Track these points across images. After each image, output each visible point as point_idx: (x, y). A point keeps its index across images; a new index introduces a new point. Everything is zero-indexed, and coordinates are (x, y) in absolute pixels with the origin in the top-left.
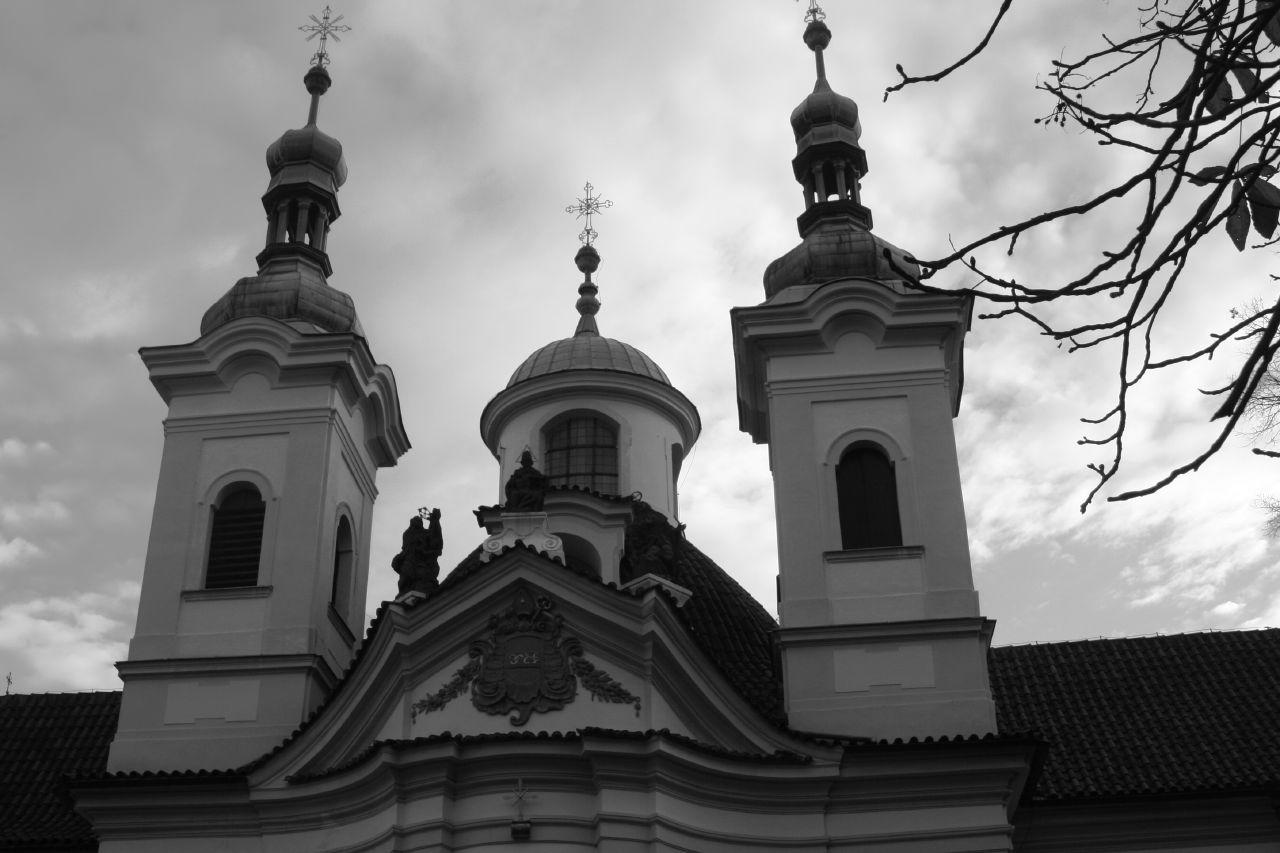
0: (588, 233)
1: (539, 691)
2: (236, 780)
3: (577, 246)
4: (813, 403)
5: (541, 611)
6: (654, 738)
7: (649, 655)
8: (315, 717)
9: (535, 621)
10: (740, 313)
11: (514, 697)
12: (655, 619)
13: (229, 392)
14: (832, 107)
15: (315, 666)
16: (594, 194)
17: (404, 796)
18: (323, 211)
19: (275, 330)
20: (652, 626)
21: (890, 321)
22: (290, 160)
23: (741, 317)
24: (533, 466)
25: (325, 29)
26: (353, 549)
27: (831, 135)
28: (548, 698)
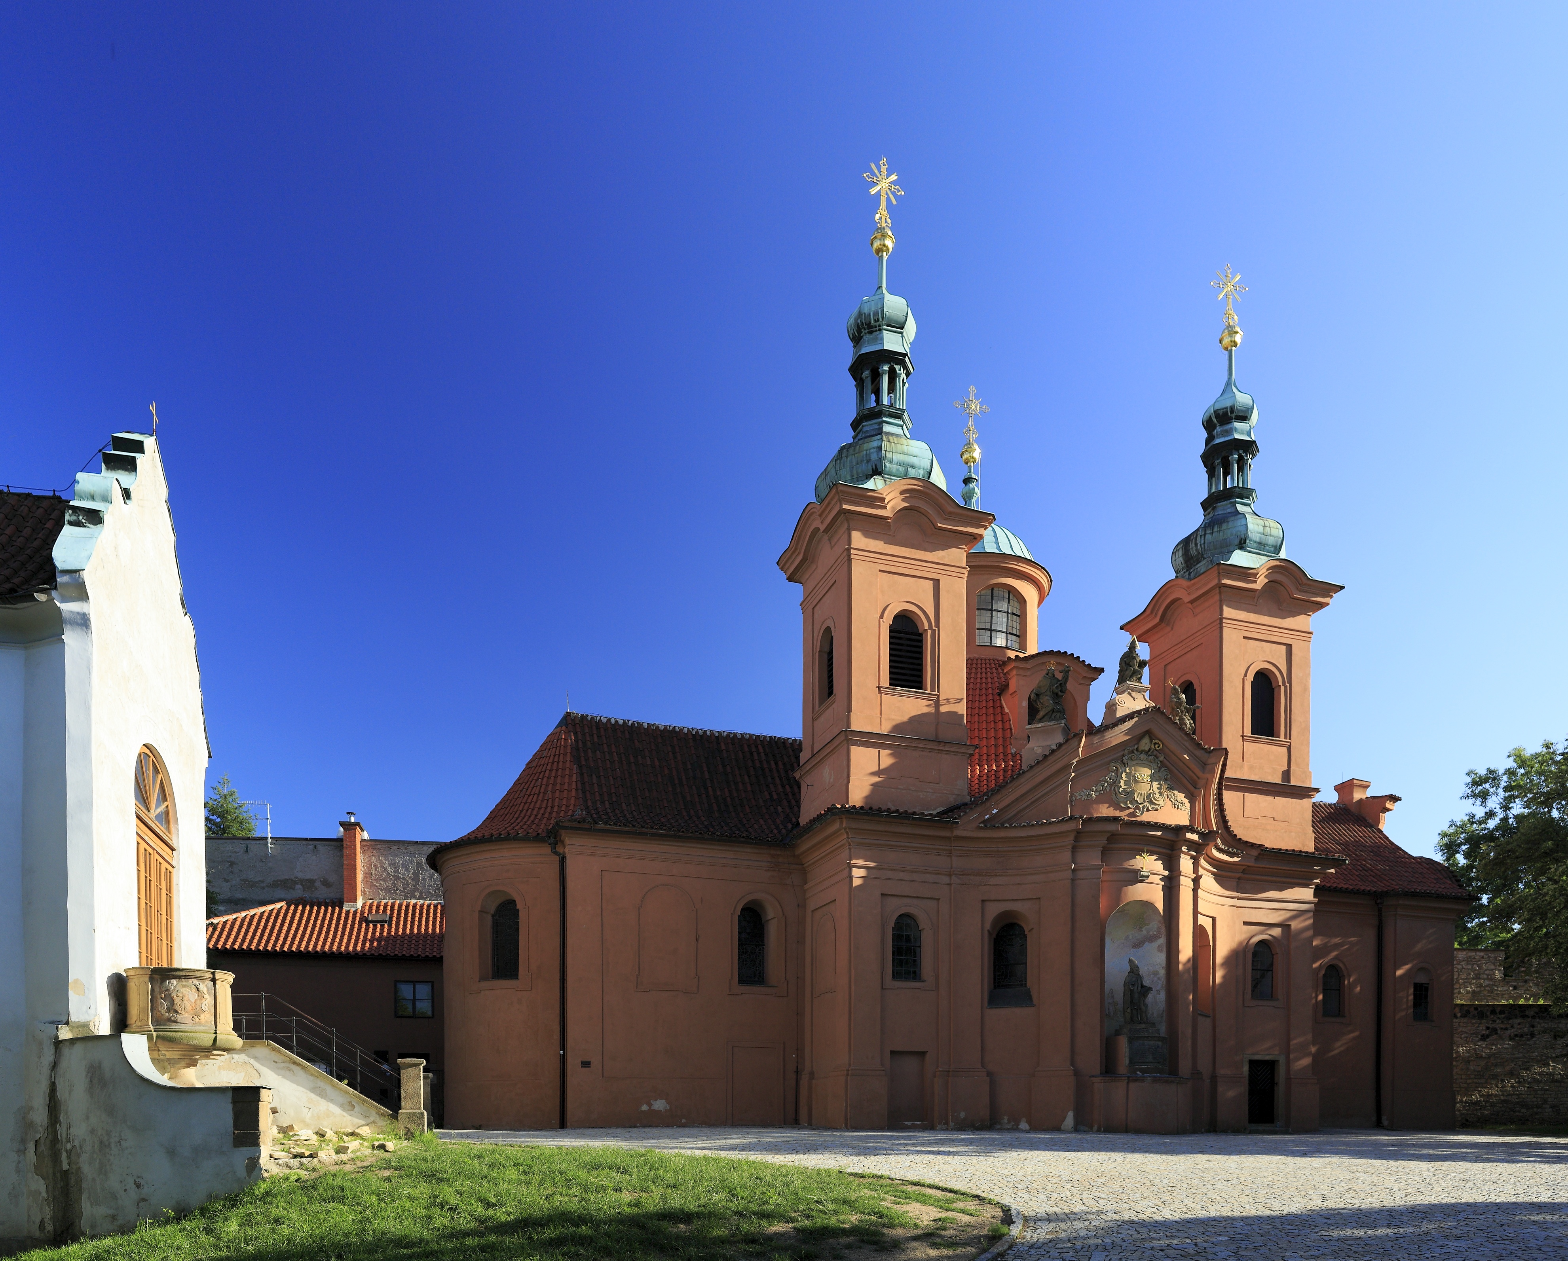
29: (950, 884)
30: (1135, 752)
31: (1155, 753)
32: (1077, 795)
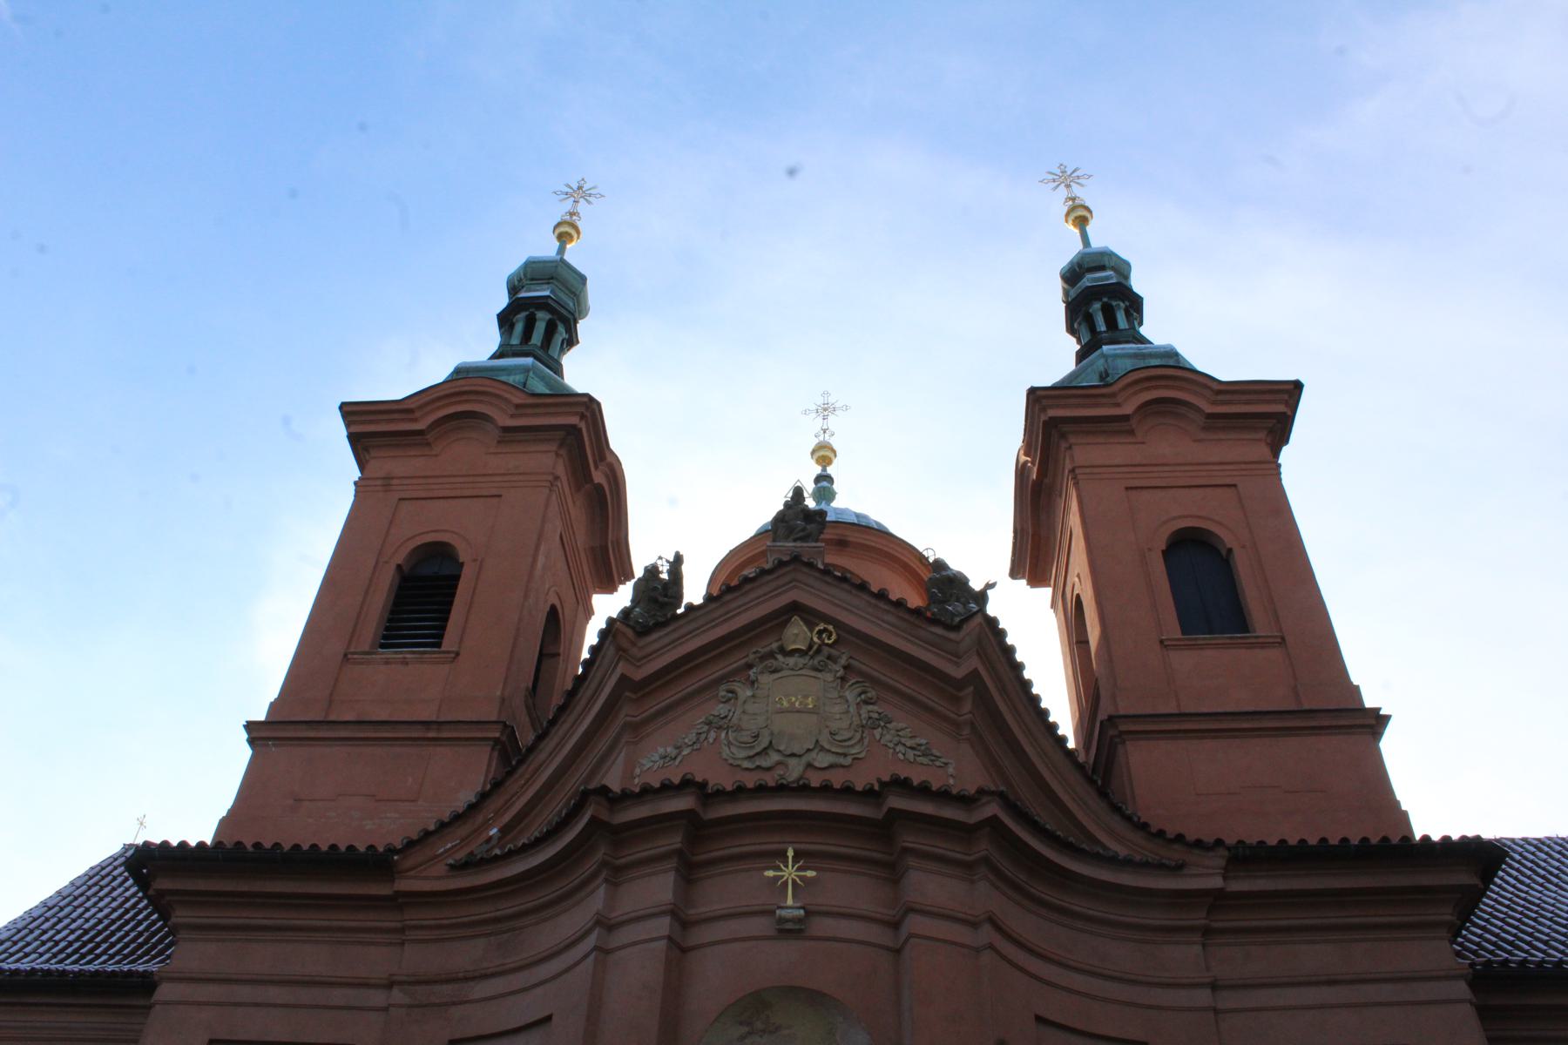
0: (825, 432)
1: (817, 741)
2: (377, 863)
3: (812, 443)
4: (1127, 488)
5: (820, 646)
6: (985, 799)
7: (967, 706)
8: (497, 785)
9: (812, 657)
10: (1039, 393)
11: (782, 748)
12: (979, 654)
13: (436, 456)
14: (1106, 258)
15: (504, 738)
16: (831, 400)
17: (616, 874)
18: (561, 333)
19: (502, 393)
20: (974, 663)
21: (1209, 409)
22: (532, 279)
23: (1036, 397)
24: (806, 503)
25: (579, 192)
26: (561, 650)
27: (1107, 278)
28: (829, 751)
29: (386, 1009)
30: (780, 657)
31: (826, 650)
32: (644, 762)
